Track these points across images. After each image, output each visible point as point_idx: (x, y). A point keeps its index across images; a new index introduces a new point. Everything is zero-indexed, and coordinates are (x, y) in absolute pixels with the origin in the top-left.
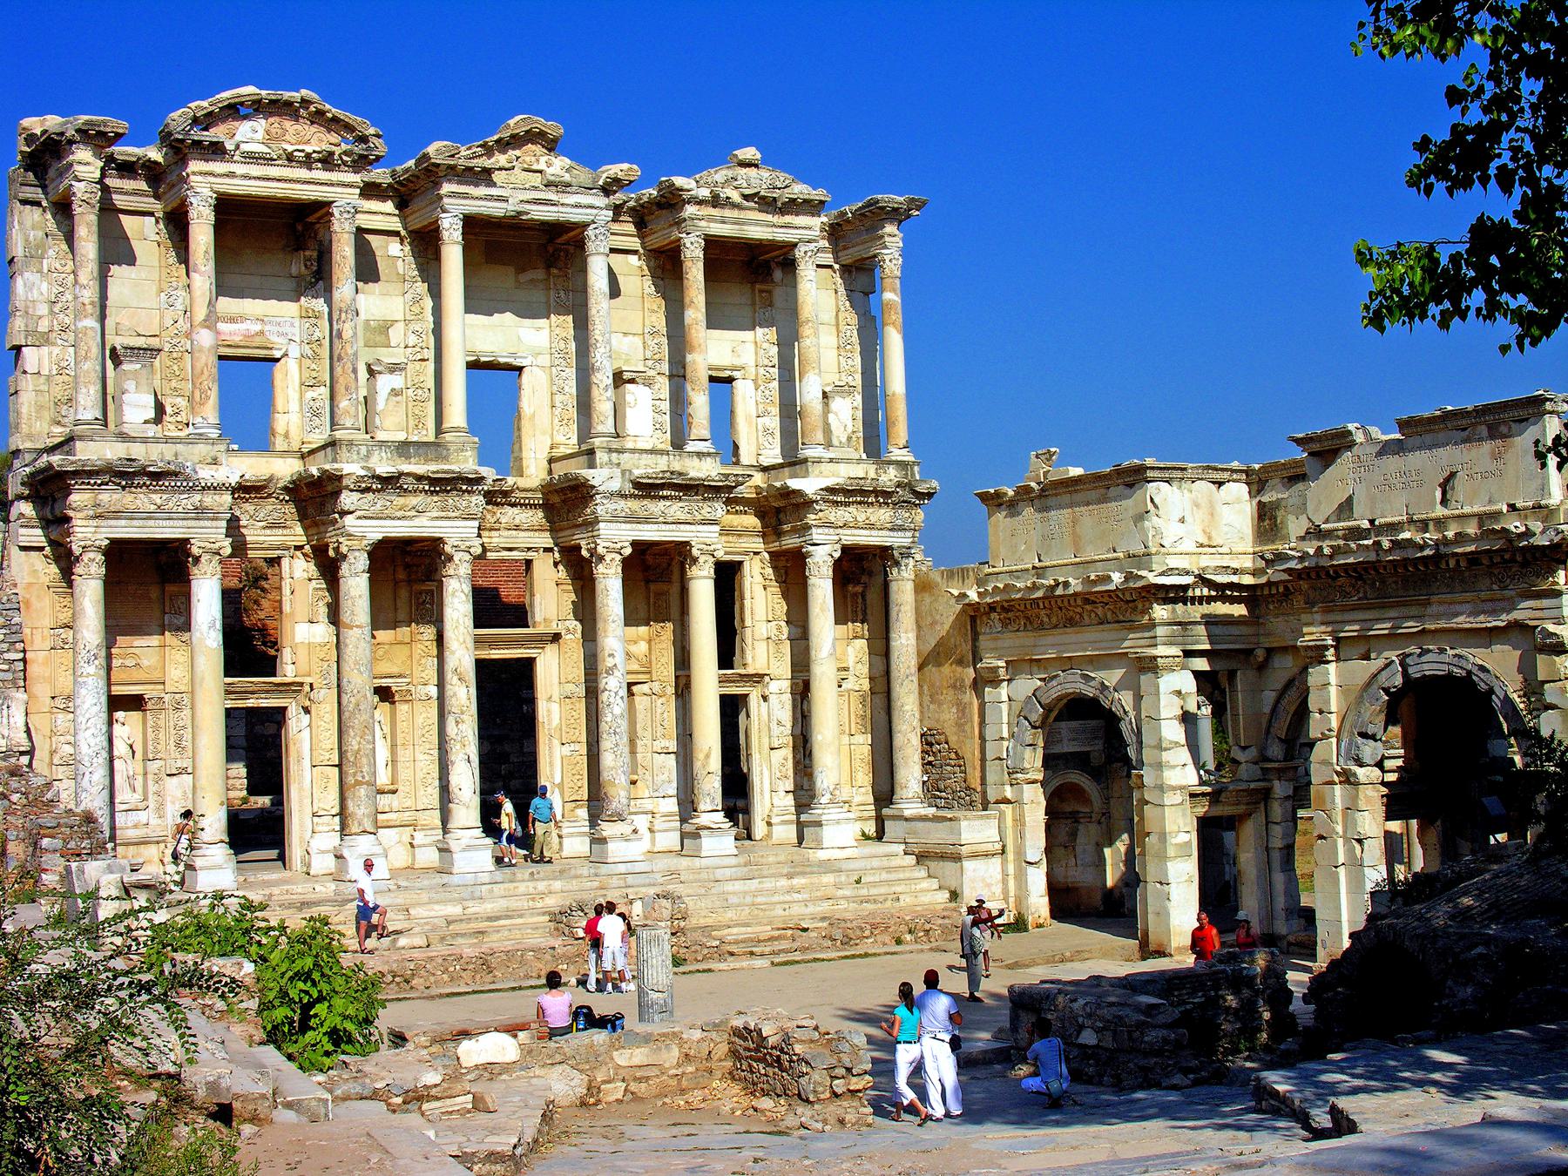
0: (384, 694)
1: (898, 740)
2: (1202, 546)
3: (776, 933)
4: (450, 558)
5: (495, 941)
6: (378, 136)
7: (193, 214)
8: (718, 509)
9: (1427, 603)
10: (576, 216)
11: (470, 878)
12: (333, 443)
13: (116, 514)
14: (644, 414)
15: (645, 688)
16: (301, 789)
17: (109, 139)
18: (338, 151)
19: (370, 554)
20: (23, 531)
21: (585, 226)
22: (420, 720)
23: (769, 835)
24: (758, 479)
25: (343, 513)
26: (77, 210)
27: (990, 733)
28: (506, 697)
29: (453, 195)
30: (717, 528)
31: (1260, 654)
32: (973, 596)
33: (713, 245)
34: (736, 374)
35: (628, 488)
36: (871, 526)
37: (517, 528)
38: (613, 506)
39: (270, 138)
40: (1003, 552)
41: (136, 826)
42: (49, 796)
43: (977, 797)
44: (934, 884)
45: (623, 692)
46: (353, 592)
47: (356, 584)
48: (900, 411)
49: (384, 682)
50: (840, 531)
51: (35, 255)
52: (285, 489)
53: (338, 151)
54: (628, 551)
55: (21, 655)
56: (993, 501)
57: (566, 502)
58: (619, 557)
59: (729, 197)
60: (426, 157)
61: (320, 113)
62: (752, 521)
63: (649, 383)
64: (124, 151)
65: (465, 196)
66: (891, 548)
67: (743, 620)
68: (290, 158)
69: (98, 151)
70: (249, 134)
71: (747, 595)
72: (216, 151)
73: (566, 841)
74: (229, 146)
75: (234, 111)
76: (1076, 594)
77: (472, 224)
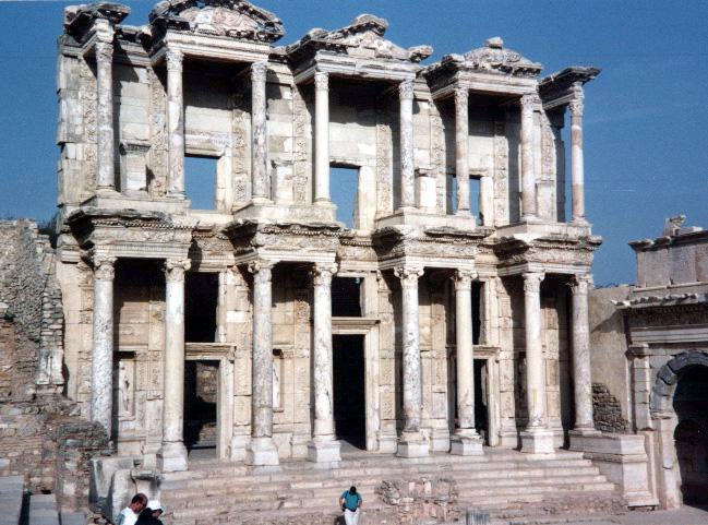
0: (277, 352)
1: (578, 389)
3: (511, 505)
4: (318, 274)
6: (280, 23)
7: (170, 65)
8: (474, 250)
11: (327, 466)
12: (251, 205)
14: (432, 190)
15: (428, 354)
16: (227, 409)
17: (118, 17)
18: (256, 31)
19: (273, 271)
20: (64, 252)
21: (399, 82)
22: (298, 369)
23: (500, 444)
24: (495, 235)
25: (257, 246)
26: (99, 60)
27: (638, 387)
28: (348, 355)
29: (323, 61)
30: (472, 261)
34: (483, 174)
35: (423, 236)
36: (563, 263)
37: (356, 259)
38: (413, 247)
39: (216, 22)
40: (647, 279)
41: (126, 431)
42: (74, 412)
43: (629, 426)
44: (603, 479)
46: (262, 293)
47: (264, 288)
48: (580, 196)
49: (278, 347)
51: (74, 87)
52: (223, 232)
53: (256, 31)
54: (422, 273)
55: (60, 327)
56: (639, 247)
57: (386, 242)
58: (416, 277)
60: (308, 37)
61: (246, 8)
62: (491, 258)
63: (434, 176)
64: (126, 27)
65: (329, 62)
67: (484, 315)
68: (228, 34)
69: (112, 23)
70: (203, 17)
71: (487, 302)
72: (184, 26)
73: (381, 443)
74: (192, 25)
76: (700, 304)
77: (335, 80)
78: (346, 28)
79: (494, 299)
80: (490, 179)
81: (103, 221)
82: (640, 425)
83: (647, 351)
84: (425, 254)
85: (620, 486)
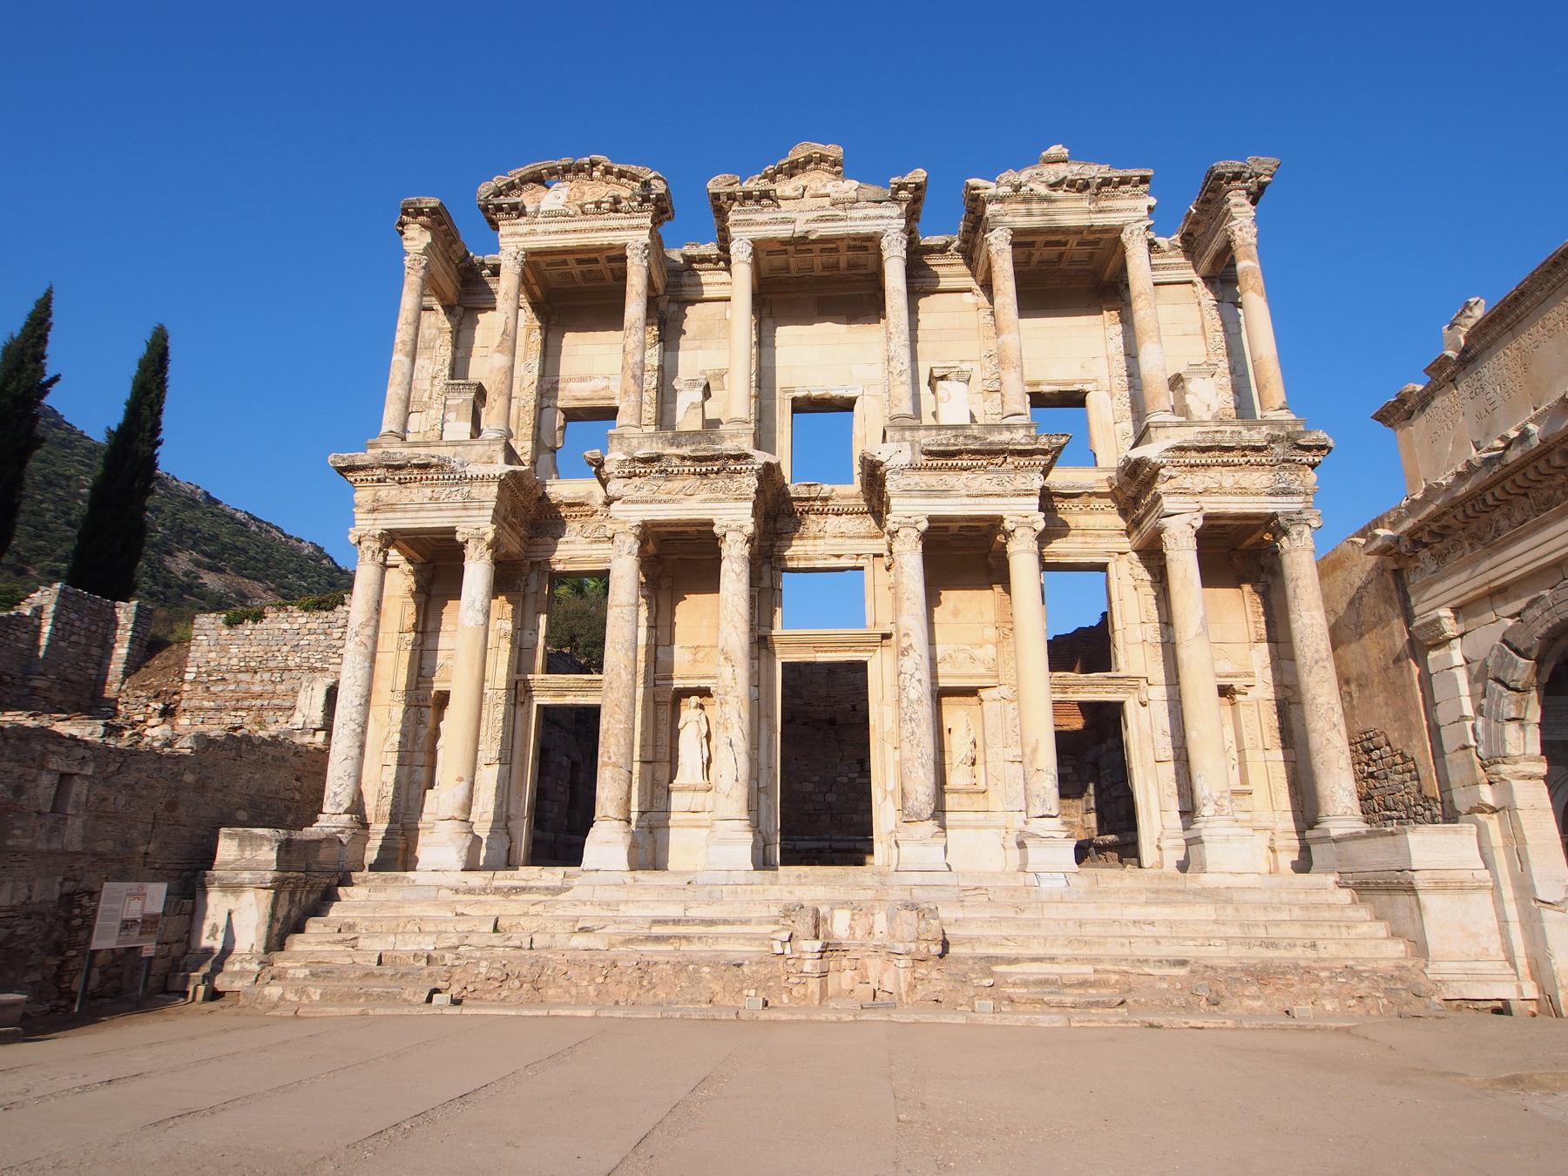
10: (866, 228)
13: (391, 507)
27: (1443, 715)
33: (1022, 241)
34: (1086, 387)
36: (1243, 491)
37: (842, 535)
44: (1381, 929)
49: (703, 683)
50: (1201, 498)
54: (924, 526)
59: (1038, 194)
65: (749, 223)
66: (1274, 516)
72: (518, 210)
74: (530, 209)
75: (539, 180)
78: (769, 169)
79: (1128, 593)
80: (1104, 395)
81: (361, 475)
82: (1461, 801)
83: (1450, 627)
84: (930, 493)
85: (1420, 948)
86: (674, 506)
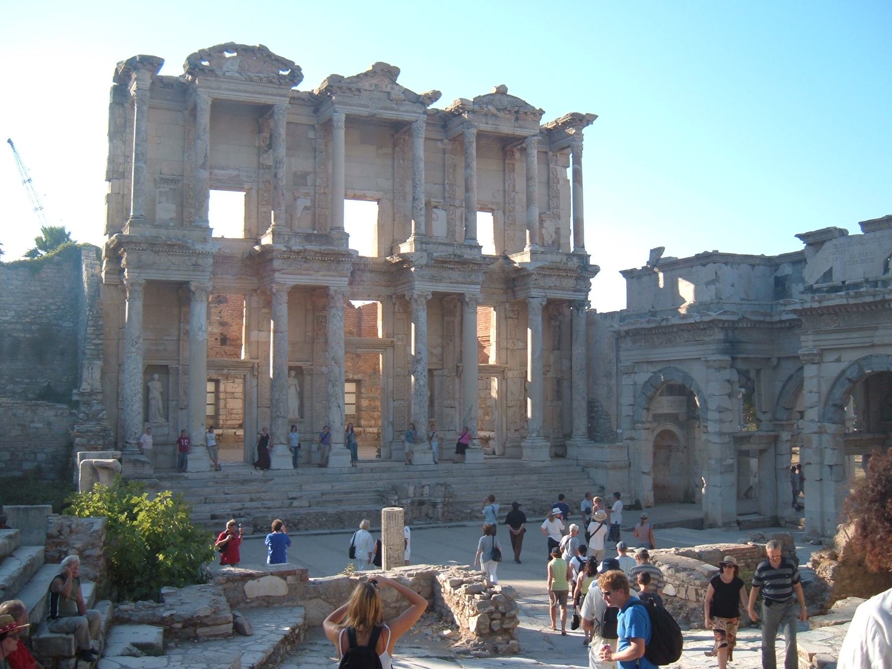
1: (575, 404)
2: (743, 300)
4: (333, 298)
5: (346, 508)
9: (876, 329)
10: (407, 117)
15: (440, 372)
25: (274, 271)
30: (479, 287)
31: (774, 361)
32: (616, 326)
34: (494, 207)
45: (426, 373)
49: (298, 364)
54: (430, 297)
73: (394, 453)
76: (673, 326)
80: (501, 212)
84: (433, 279)
86: (309, 277)
